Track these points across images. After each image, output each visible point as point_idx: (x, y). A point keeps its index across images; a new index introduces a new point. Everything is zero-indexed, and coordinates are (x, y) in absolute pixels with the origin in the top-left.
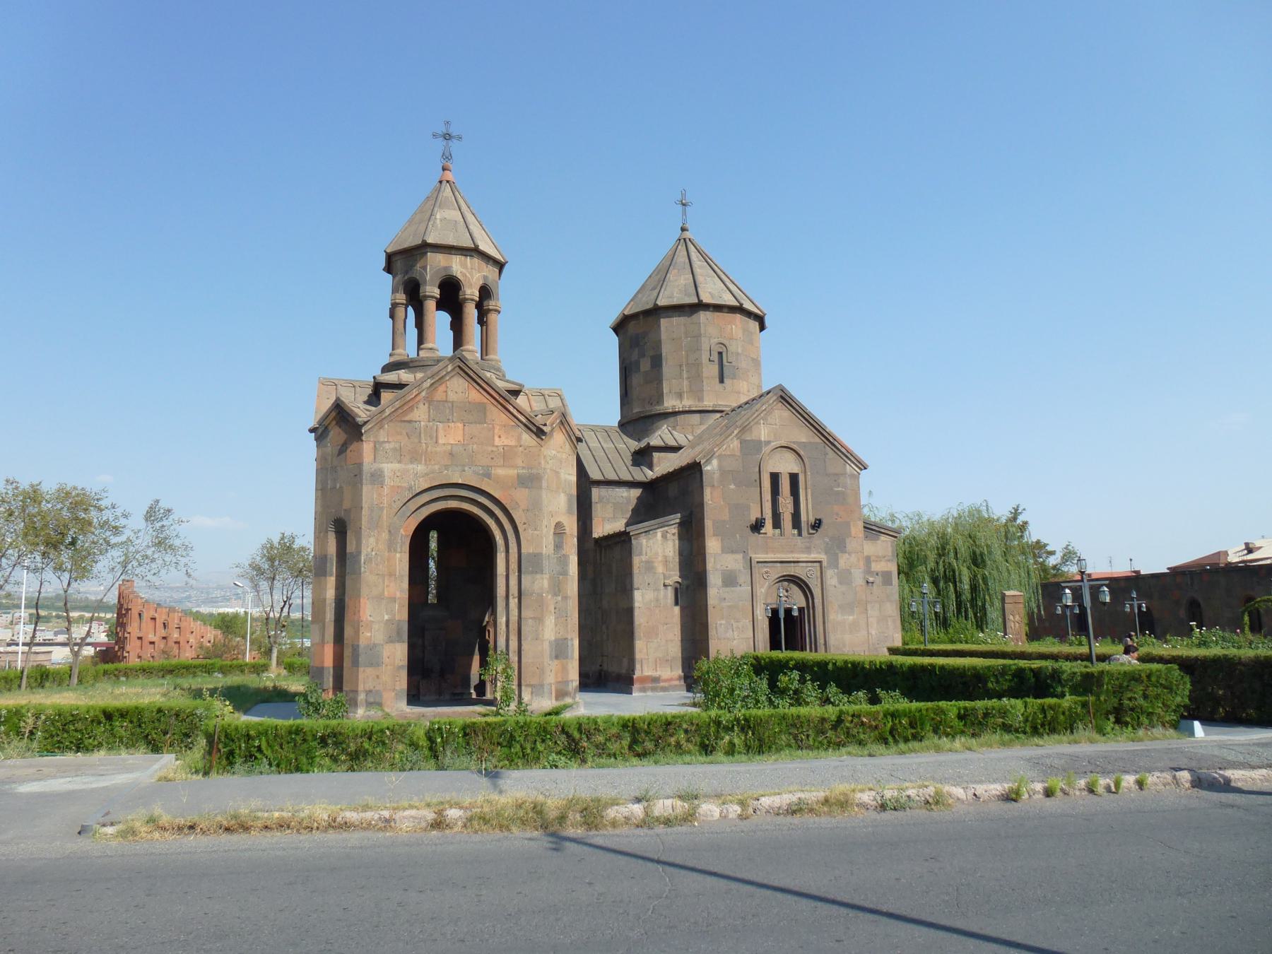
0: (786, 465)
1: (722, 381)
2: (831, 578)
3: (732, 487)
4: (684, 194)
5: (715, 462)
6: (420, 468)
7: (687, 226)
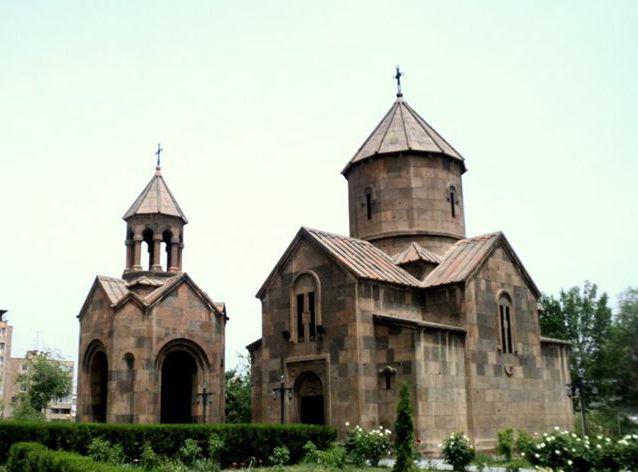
0: (305, 289)
1: (369, 217)
2: (332, 372)
3: (276, 311)
4: (398, 70)
5: (267, 296)
6: (88, 334)
7: (402, 92)
